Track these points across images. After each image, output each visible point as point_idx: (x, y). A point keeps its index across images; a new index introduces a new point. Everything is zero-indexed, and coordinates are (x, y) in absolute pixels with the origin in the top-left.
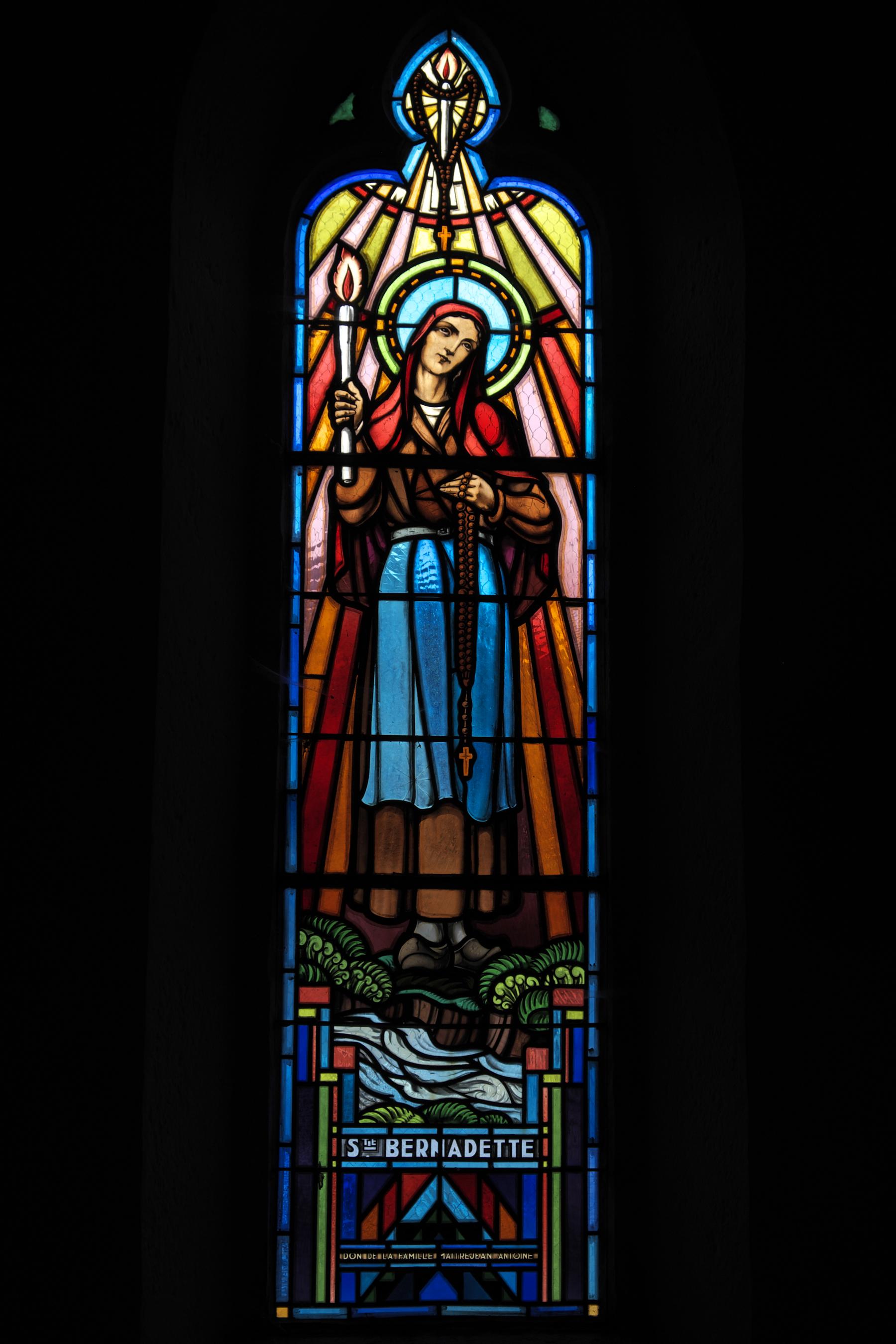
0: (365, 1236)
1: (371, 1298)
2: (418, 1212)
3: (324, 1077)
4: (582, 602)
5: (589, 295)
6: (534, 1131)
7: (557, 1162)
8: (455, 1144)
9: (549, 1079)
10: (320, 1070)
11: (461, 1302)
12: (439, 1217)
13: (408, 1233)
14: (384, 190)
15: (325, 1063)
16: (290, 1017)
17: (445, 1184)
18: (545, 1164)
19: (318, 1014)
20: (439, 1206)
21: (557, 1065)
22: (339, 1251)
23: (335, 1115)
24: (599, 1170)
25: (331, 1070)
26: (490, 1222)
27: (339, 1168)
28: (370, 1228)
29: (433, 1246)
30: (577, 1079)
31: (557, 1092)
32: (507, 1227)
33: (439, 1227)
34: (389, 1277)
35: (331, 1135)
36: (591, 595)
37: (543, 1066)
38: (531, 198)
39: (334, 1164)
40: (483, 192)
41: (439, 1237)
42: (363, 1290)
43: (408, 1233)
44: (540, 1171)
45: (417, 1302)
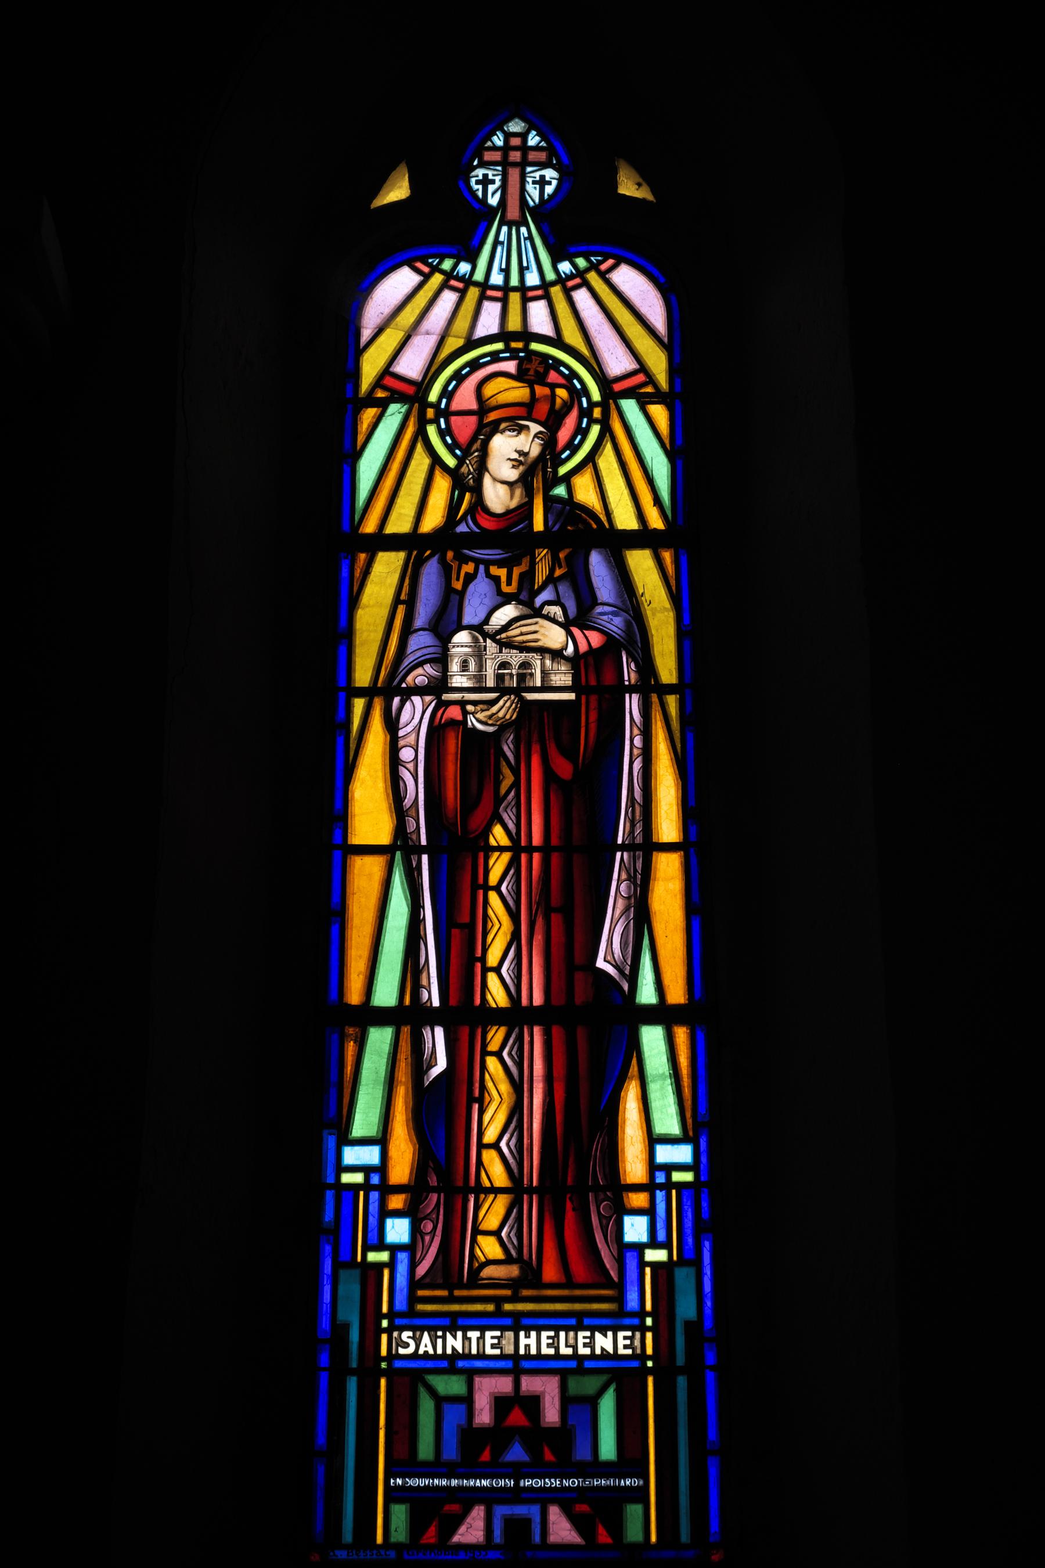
14: (447, 265)
16: (330, 1180)
19: (367, 1178)
21: (661, 1236)
25: (381, 1246)
37: (644, 1238)
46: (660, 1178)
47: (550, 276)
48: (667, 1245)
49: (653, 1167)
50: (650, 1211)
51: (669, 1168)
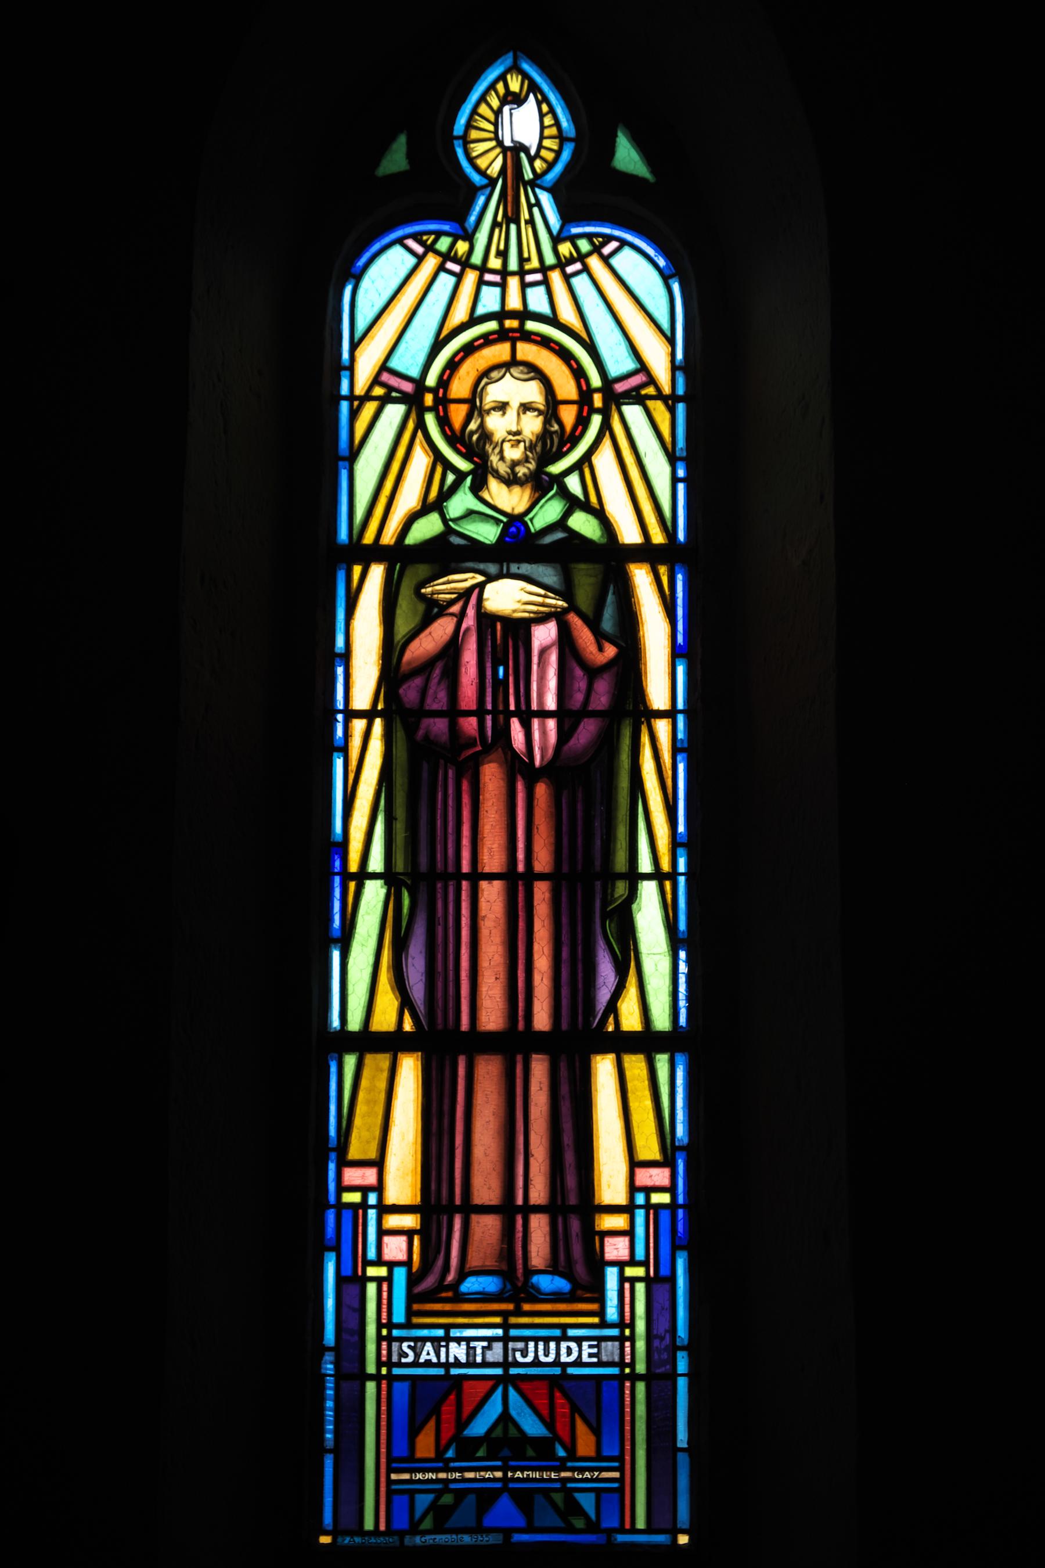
0: (419, 1454)
1: (427, 1524)
2: (479, 1427)
3: (371, 1272)
4: (671, 714)
5: (680, 355)
6: (615, 1332)
7: (641, 1368)
8: (428, 1346)
9: (630, 1272)
10: (367, 1263)
11: (530, 1529)
12: (506, 1430)
13: (468, 1449)
15: (372, 1254)
16: (332, 1199)
17: (512, 1392)
18: (627, 1371)
20: (505, 1417)
21: (640, 1254)
22: (390, 1470)
23: (384, 1315)
24: (692, 1375)
25: (379, 1262)
26: (567, 1439)
27: (391, 1378)
28: (425, 1445)
29: (499, 1463)
30: (664, 1271)
31: (640, 1288)
32: (585, 1443)
33: (506, 1443)
34: (447, 1499)
35: (380, 1338)
36: (680, 705)
38: (614, 245)
39: (384, 1371)
40: (556, 240)
41: (506, 1452)
42: (418, 1514)
43: (468, 1449)
44: (621, 1378)
45: (479, 1529)
46: (640, 1199)
47: (550, 259)
48: (645, 1264)
49: (633, 1189)
50: (629, 1233)
51: (648, 1190)
